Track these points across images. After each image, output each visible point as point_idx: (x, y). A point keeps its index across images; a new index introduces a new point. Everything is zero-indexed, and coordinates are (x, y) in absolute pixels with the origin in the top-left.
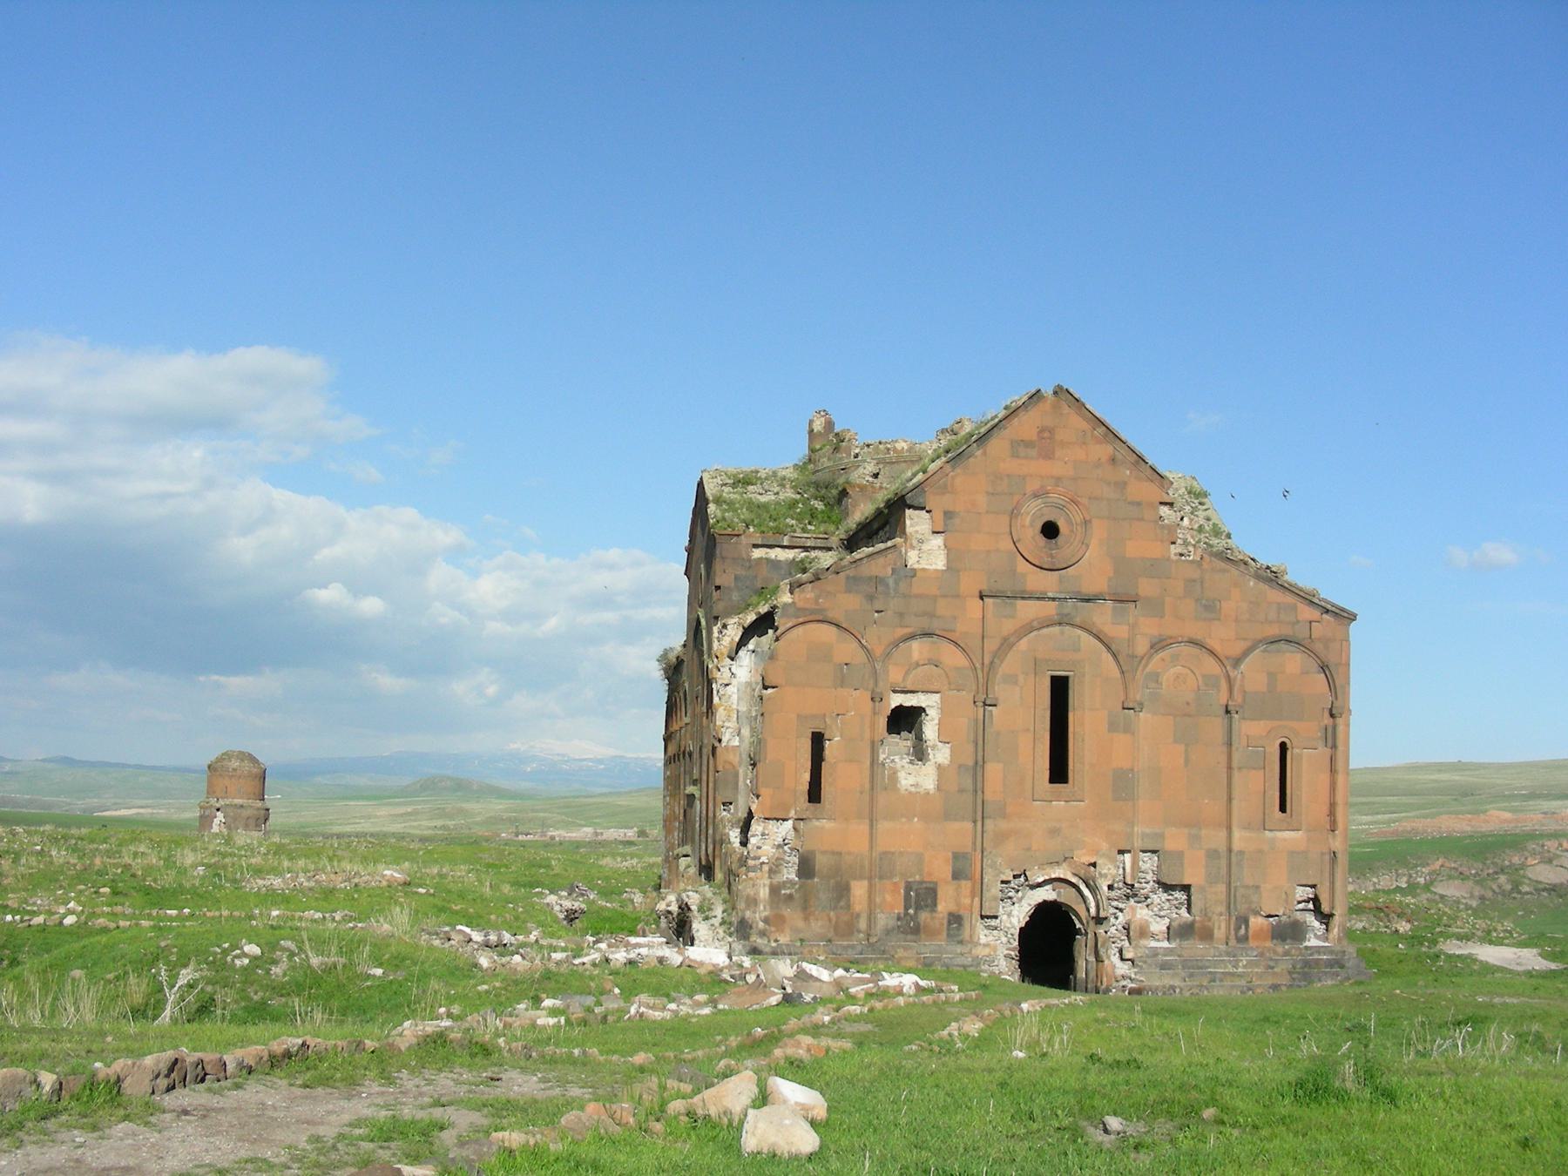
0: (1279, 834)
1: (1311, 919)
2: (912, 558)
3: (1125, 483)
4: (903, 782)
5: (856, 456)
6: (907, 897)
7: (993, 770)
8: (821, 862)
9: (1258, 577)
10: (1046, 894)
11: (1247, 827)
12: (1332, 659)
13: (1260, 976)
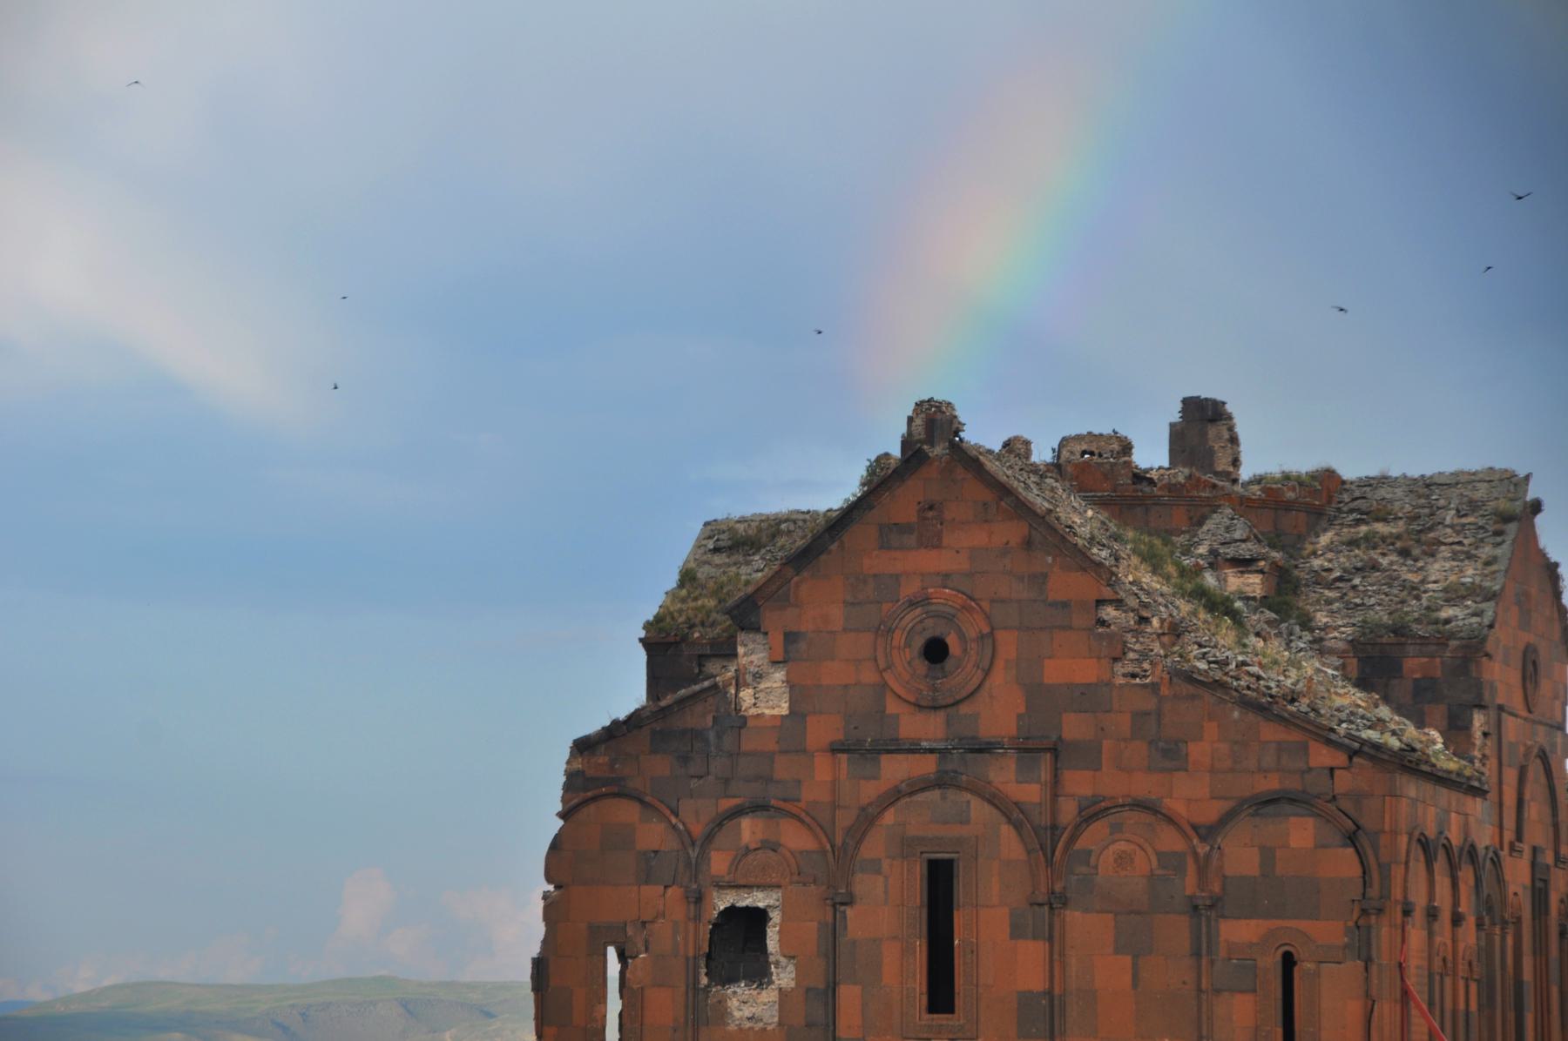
3: (1045, 576)
7: (848, 994)
9: (1247, 704)
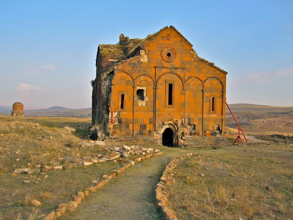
0: (212, 115)
1: (218, 132)
2: (141, 60)
4: (140, 104)
5: (129, 42)
6: (140, 127)
8: (124, 120)
10: (167, 127)
11: (206, 114)
12: (223, 81)
13: (209, 142)
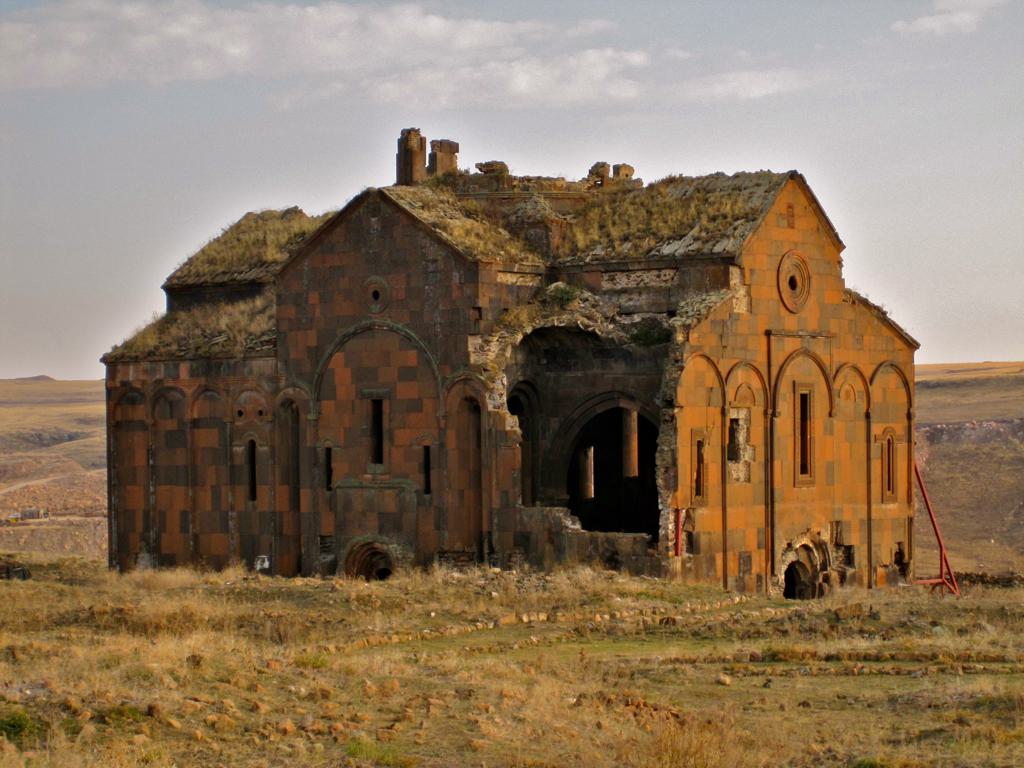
7: (777, 463)
